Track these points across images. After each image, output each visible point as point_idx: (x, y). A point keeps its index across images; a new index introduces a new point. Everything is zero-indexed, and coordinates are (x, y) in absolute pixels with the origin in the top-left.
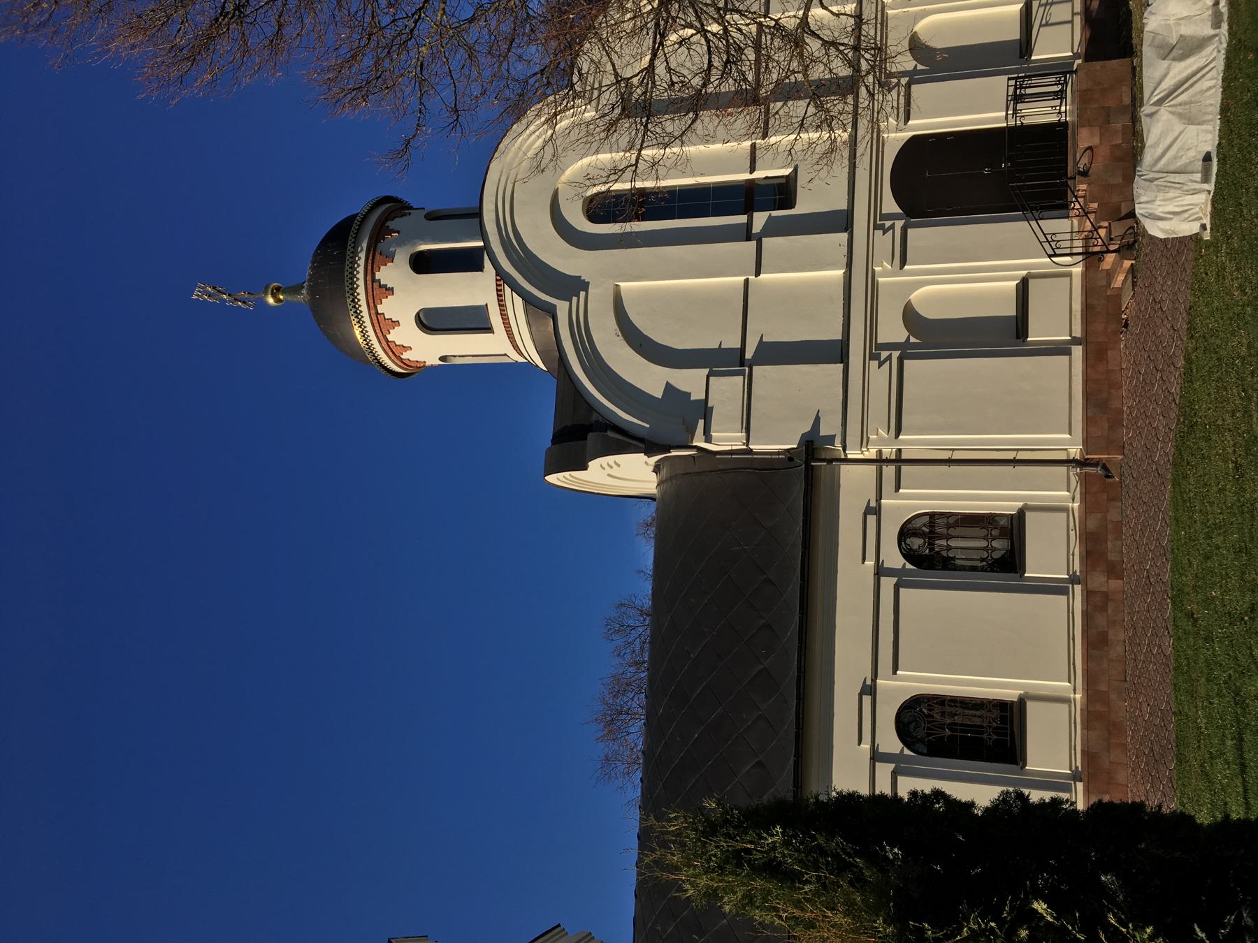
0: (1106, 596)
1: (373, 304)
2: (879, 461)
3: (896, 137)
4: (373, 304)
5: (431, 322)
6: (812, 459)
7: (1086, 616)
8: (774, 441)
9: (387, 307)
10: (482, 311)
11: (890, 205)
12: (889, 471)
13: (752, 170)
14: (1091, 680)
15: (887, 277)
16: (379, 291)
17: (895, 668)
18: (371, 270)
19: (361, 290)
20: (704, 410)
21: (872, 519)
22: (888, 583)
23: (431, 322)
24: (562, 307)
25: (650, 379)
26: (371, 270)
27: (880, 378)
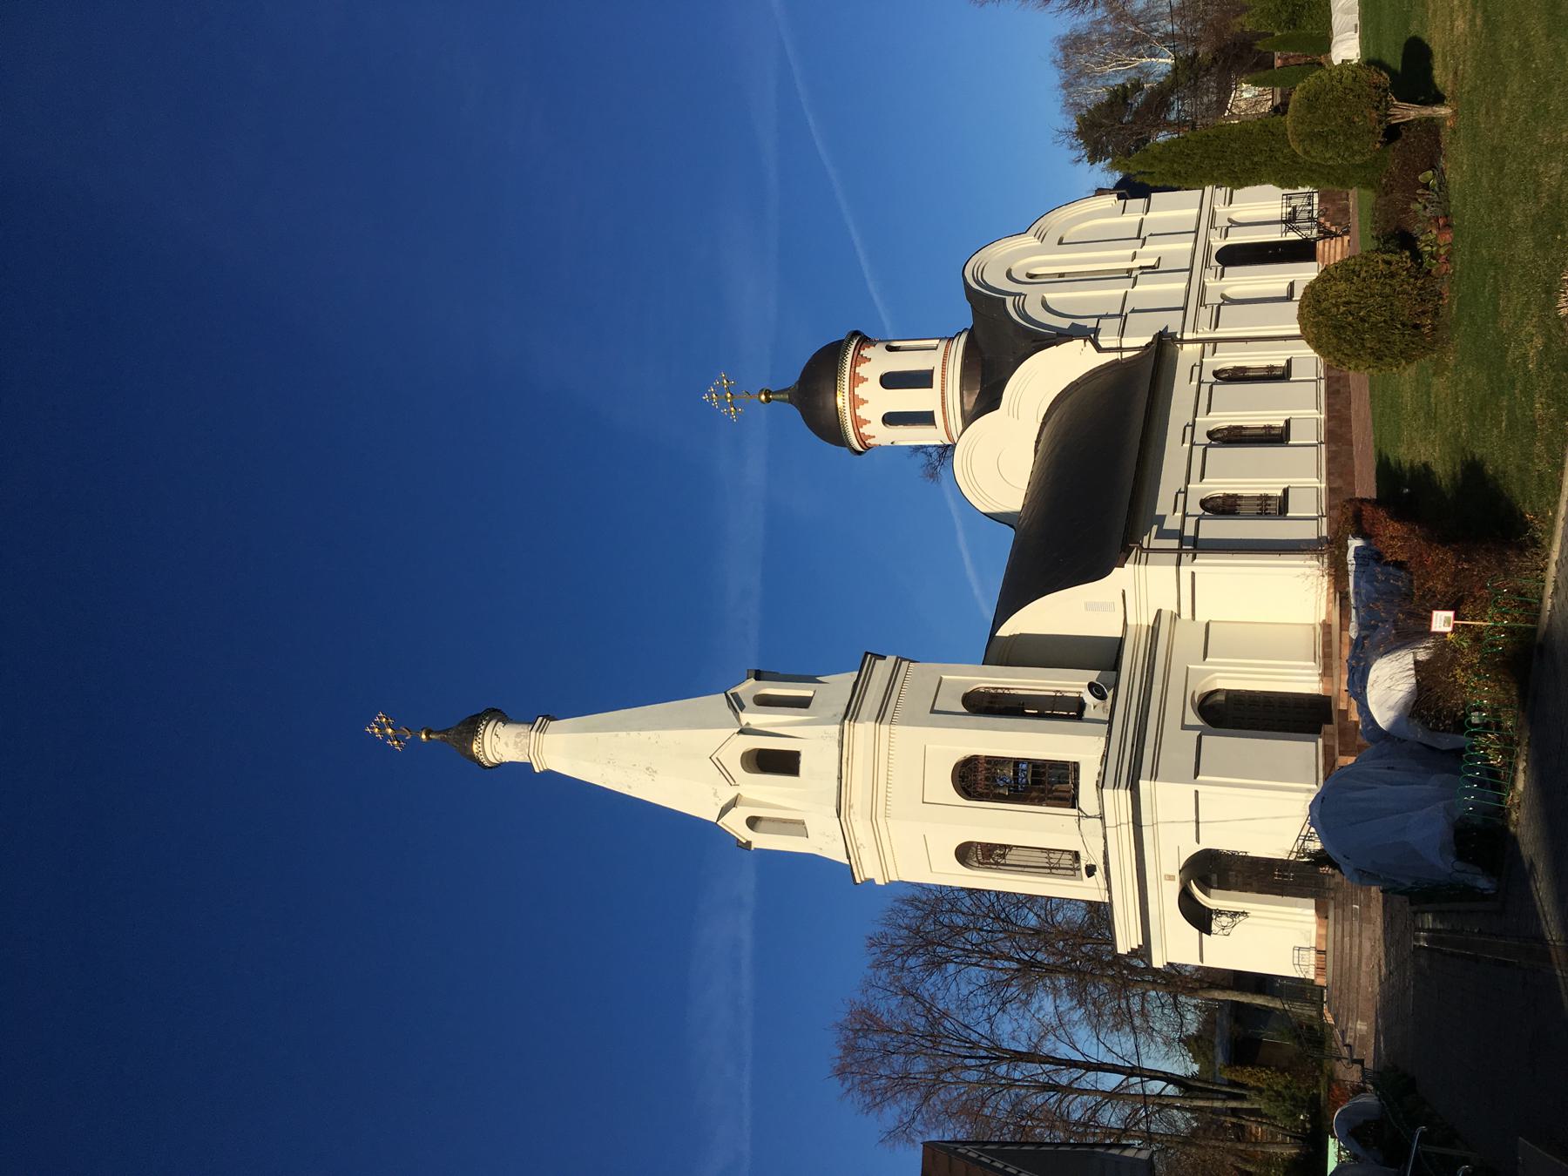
0: (1339, 379)
1: (854, 365)
2: (1203, 341)
3: (1218, 243)
4: (854, 365)
5: (891, 381)
6: (1163, 347)
7: (1328, 387)
8: (1137, 340)
9: (862, 370)
10: (932, 371)
11: (1214, 262)
12: (1209, 347)
13: (1134, 256)
14: (1329, 407)
15: (1211, 282)
16: (858, 360)
17: (1209, 411)
18: (859, 348)
19: (849, 356)
20: (1096, 331)
21: (1196, 370)
22: (1205, 389)
23: (891, 381)
24: (1009, 300)
25: (1064, 324)
26: (859, 348)
27: (1205, 314)
